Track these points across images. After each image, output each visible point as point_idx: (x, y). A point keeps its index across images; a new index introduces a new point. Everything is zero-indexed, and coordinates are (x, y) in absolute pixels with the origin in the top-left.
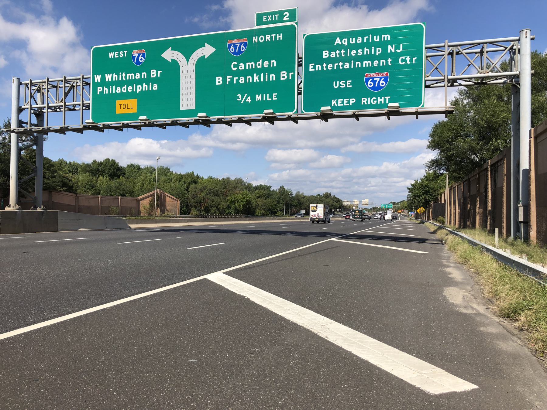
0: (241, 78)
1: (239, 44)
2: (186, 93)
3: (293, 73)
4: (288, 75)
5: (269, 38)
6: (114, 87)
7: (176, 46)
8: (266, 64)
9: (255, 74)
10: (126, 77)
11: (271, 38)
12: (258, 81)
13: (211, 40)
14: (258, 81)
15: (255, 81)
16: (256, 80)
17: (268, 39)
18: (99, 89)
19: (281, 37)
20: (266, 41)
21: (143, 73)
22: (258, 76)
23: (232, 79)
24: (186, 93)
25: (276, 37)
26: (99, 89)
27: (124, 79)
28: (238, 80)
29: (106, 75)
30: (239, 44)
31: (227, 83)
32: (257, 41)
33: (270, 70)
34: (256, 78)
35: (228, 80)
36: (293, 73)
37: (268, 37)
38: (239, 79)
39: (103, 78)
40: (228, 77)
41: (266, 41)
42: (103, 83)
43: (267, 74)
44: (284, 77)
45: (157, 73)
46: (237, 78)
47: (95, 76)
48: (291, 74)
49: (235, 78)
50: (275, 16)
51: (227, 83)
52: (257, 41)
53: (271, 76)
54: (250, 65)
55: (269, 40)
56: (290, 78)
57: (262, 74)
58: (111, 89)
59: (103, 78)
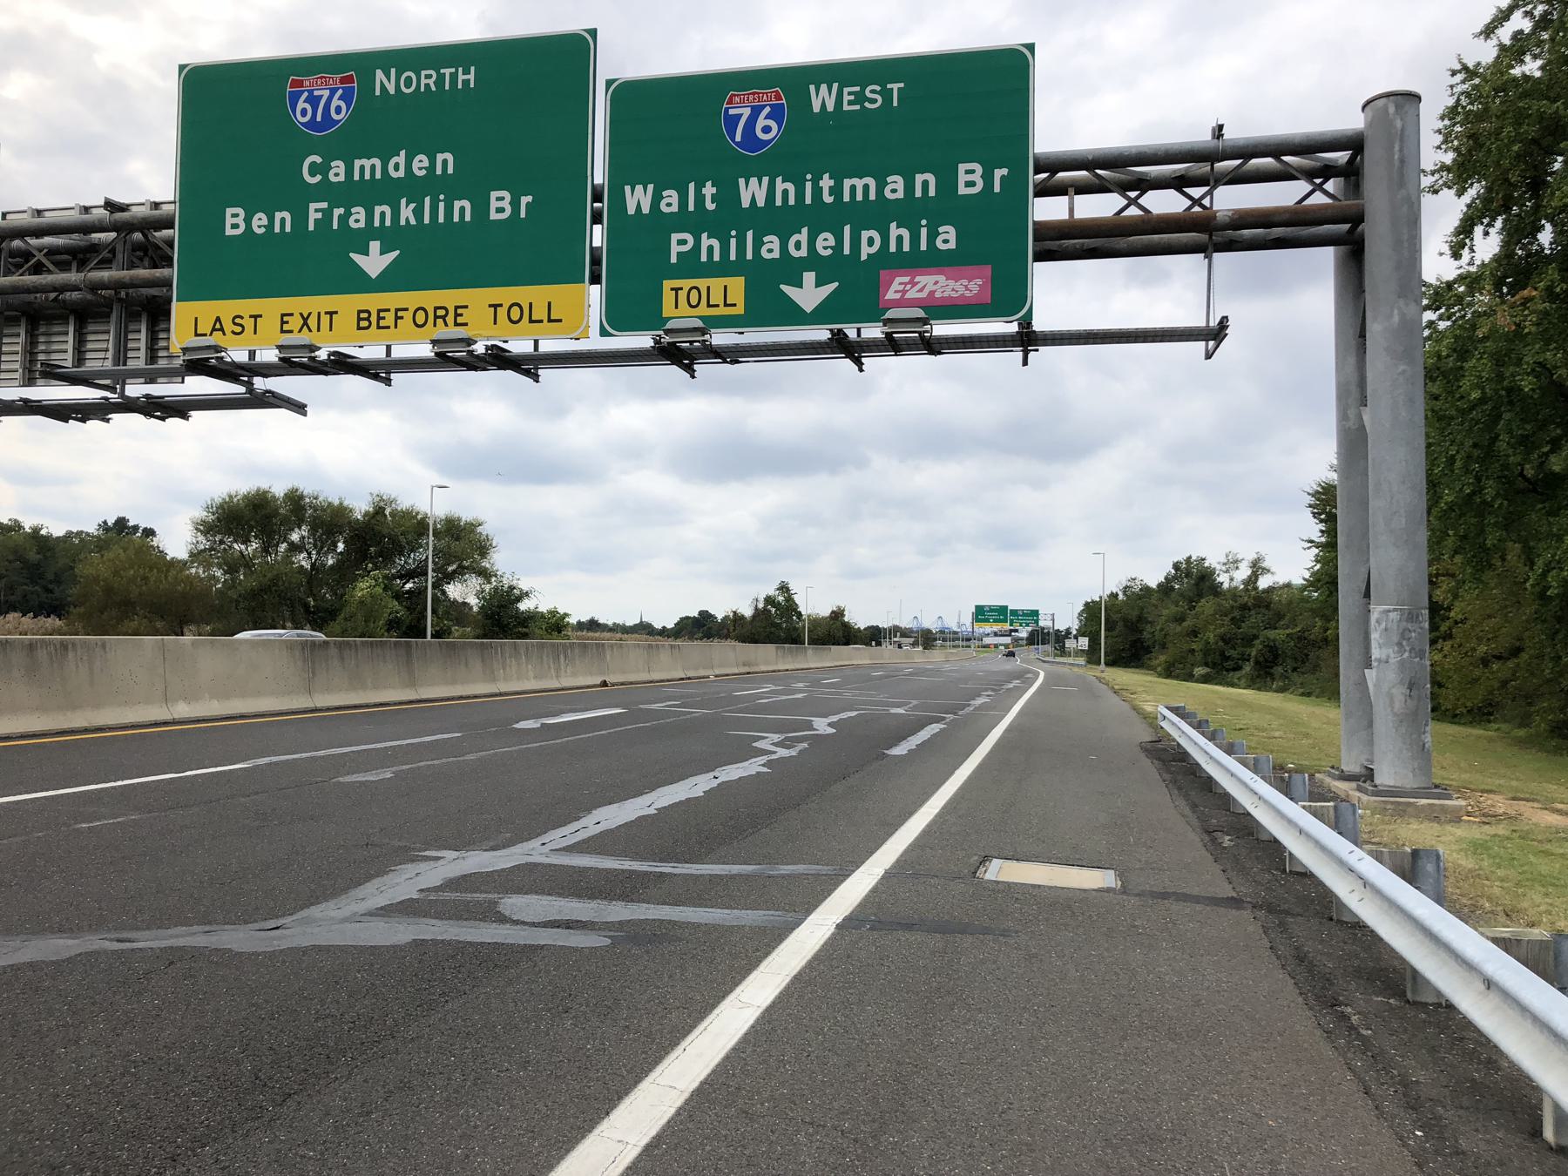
0: (353, 210)
5: (431, 82)
9: (403, 201)
11: (440, 80)
12: (413, 222)
14: (413, 222)
16: (407, 219)
17: (427, 85)
19: (471, 77)
23: (327, 214)
25: (454, 77)
28: (344, 219)
32: (391, 90)
34: (407, 213)
35: (313, 216)
38: (348, 214)
40: (313, 206)
44: (500, 210)
46: (342, 211)
49: (338, 212)
51: (311, 227)
53: (457, 204)
57: (427, 200)
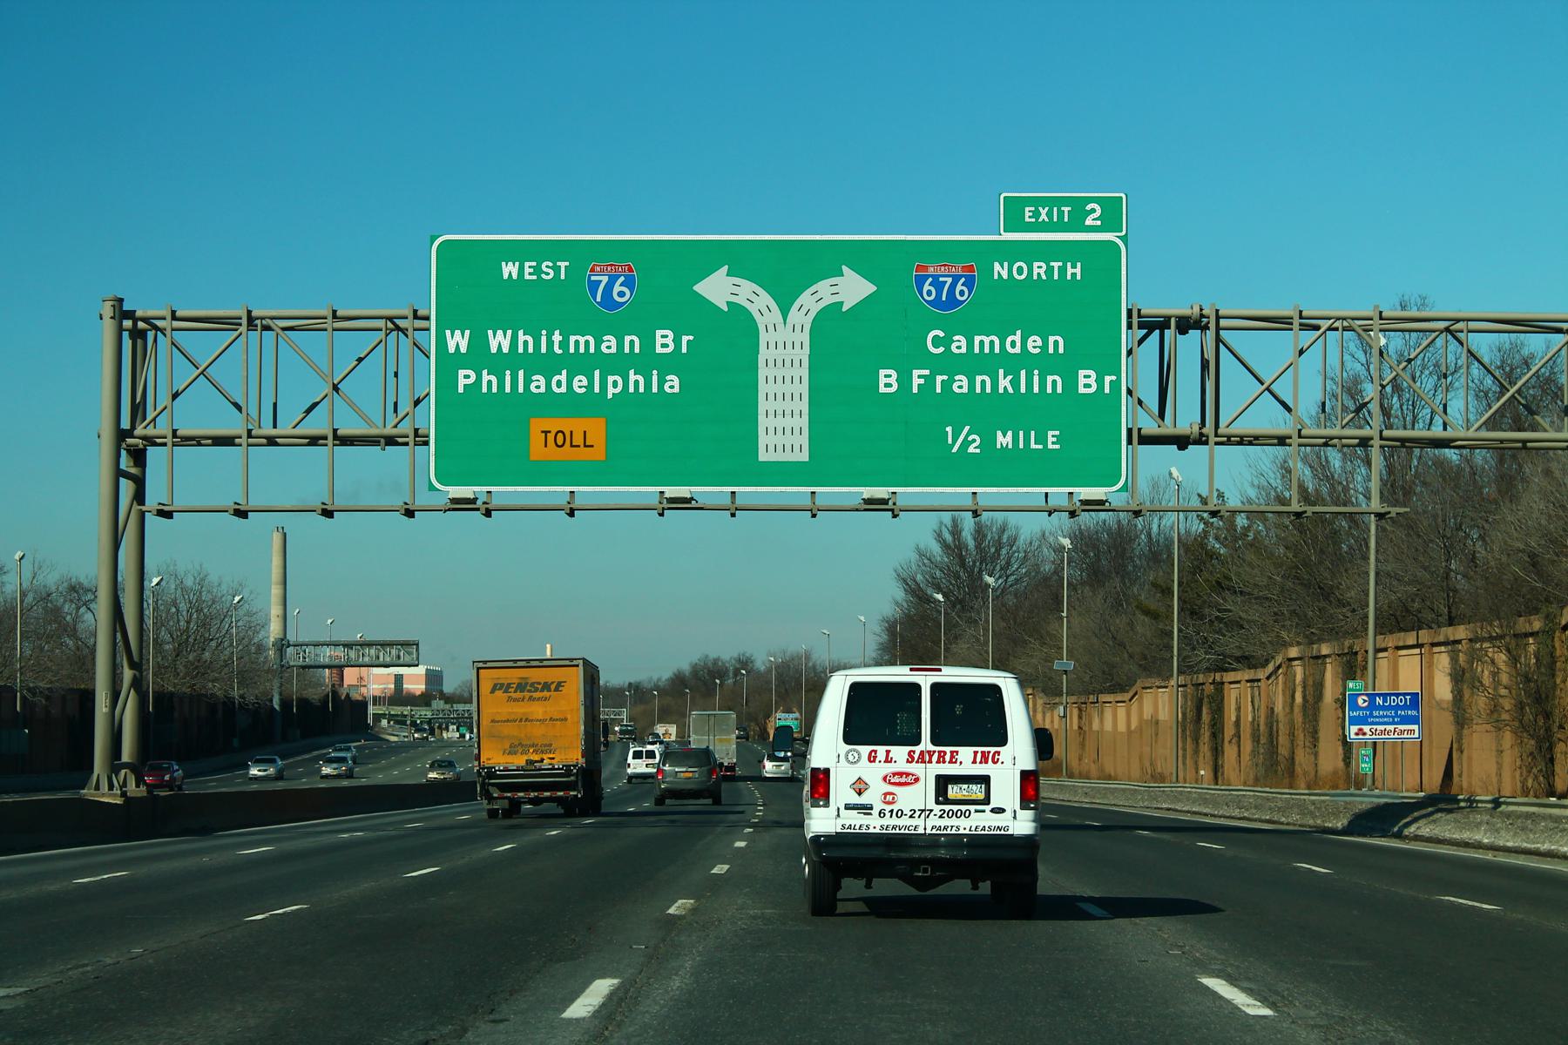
1: (951, 279)
2: (788, 412)
3: (1114, 378)
4: (1100, 381)
5: (1042, 272)
6: (521, 373)
7: (742, 260)
8: (1034, 343)
9: (1001, 372)
10: (564, 344)
12: (1011, 390)
13: (862, 258)
14: (1011, 390)
15: (1001, 391)
17: (1039, 273)
18: (465, 378)
19: (1078, 271)
20: (1035, 277)
21: (627, 339)
22: (1011, 377)
23: (930, 380)
24: (788, 412)
25: (1063, 270)
26: (465, 378)
27: (557, 350)
29: (490, 332)
30: (951, 279)
31: (915, 390)
32: (1005, 276)
33: (1046, 363)
34: (1004, 383)
35: (916, 382)
36: (1114, 378)
37: (1039, 269)
38: (952, 381)
39: (478, 343)
40: (916, 373)
41: (1035, 277)
42: (478, 356)
43: (1036, 372)
45: (677, 341)
46: (945, 377)
47: (448, 332)
48: (1108, 379)
49: (939, 379)
50: (1059, 209)
51: (915, 390)
52: (1005, 276)
53: (1050, 379)
54: (985, 341)
55: (1044, 277)
56: (1107, 390)
57: (1023, 373)
58: (508, 378)
59: (478, 343)
